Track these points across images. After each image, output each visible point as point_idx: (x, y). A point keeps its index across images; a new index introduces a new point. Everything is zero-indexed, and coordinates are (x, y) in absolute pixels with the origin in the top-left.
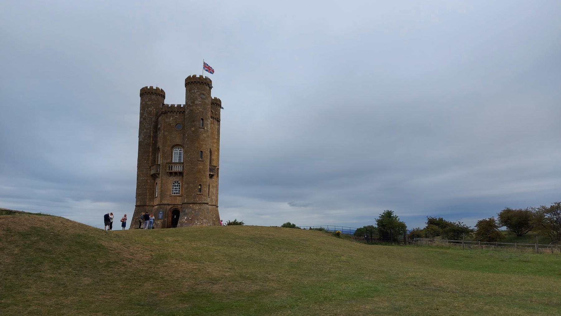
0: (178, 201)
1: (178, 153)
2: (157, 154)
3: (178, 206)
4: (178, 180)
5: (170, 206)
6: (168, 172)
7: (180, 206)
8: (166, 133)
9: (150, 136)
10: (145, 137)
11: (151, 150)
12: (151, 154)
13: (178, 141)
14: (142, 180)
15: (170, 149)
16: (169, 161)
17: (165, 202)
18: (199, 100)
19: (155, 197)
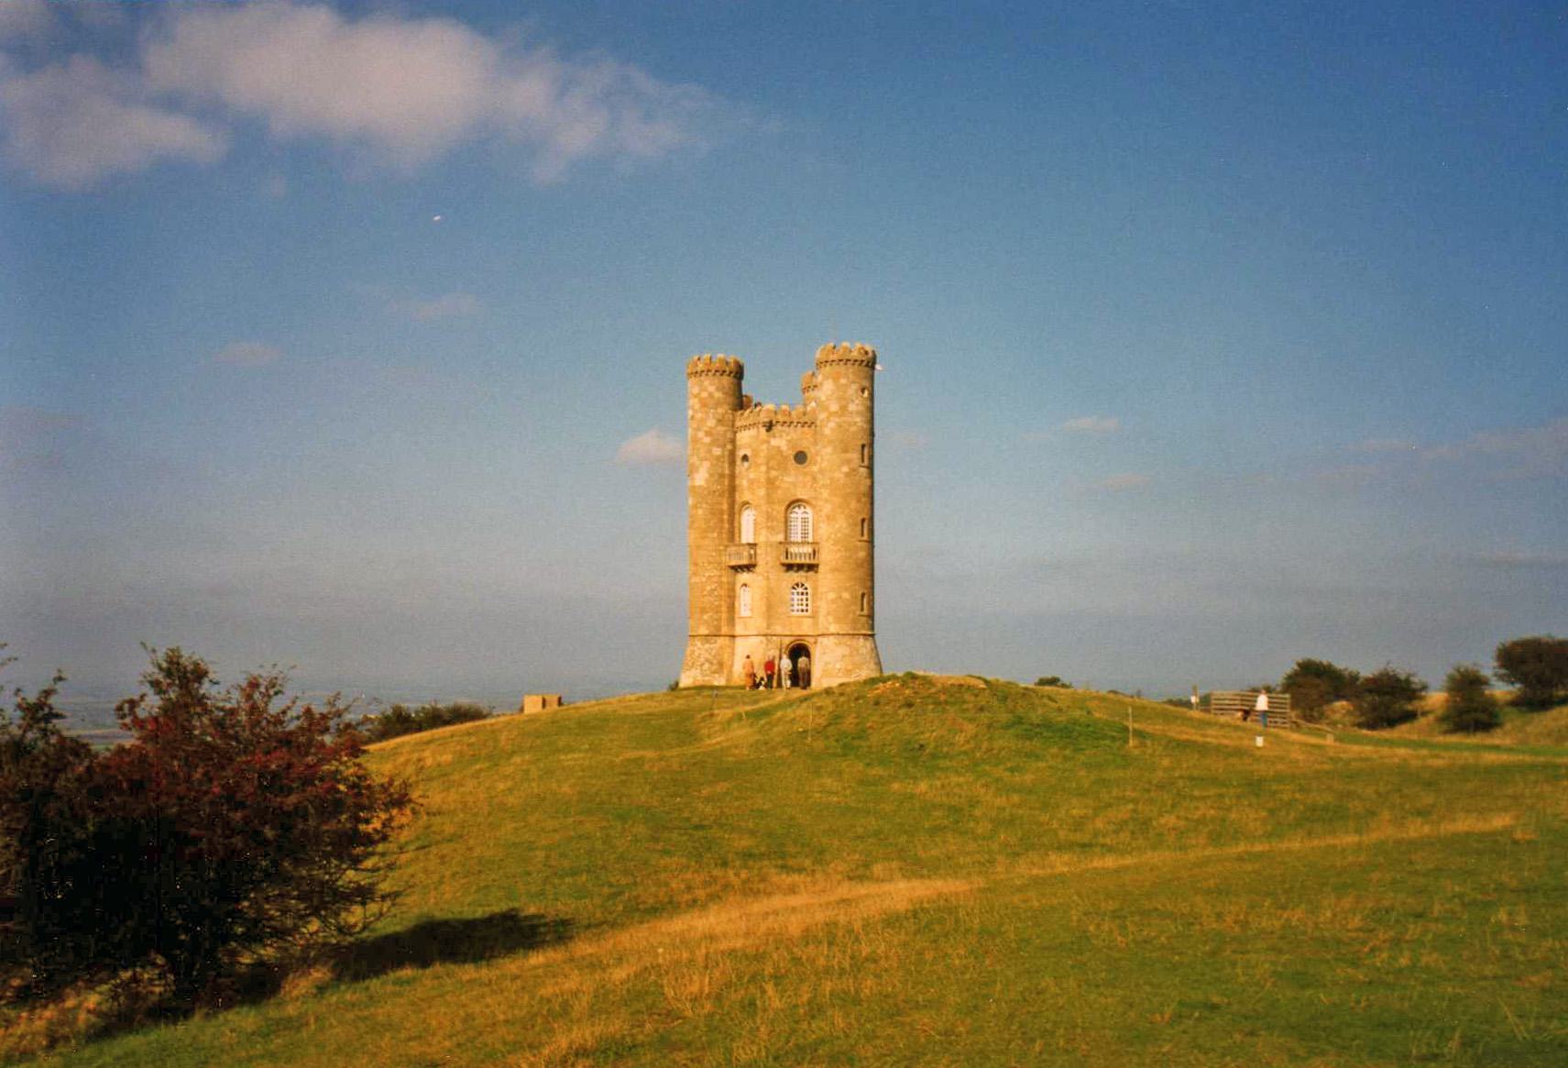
0: (805, 628)
1: (800, 520)
2: (737, 516)
3: (807, 639)
4: (803, 581)
5: (793, 639)
6: (783, 565)
7: (812, 640)
8: (773, 473)
9: (722, 476)
10: (711, 475)
11: (725, 507)
12: (726, 517)
13: (801, 494)
14: (710, 577)
15: (783, 508)
16: (781, 537)
17: (778, 629)
18: (857, 402)
19: (736, 616)
